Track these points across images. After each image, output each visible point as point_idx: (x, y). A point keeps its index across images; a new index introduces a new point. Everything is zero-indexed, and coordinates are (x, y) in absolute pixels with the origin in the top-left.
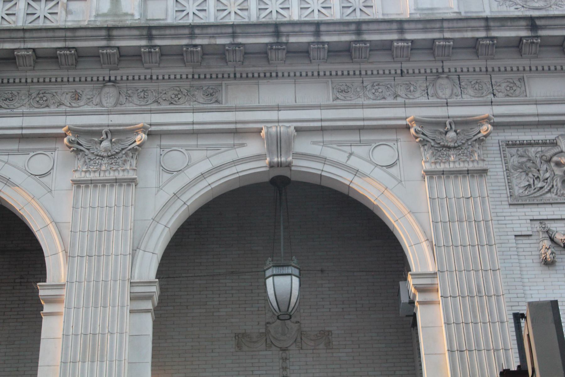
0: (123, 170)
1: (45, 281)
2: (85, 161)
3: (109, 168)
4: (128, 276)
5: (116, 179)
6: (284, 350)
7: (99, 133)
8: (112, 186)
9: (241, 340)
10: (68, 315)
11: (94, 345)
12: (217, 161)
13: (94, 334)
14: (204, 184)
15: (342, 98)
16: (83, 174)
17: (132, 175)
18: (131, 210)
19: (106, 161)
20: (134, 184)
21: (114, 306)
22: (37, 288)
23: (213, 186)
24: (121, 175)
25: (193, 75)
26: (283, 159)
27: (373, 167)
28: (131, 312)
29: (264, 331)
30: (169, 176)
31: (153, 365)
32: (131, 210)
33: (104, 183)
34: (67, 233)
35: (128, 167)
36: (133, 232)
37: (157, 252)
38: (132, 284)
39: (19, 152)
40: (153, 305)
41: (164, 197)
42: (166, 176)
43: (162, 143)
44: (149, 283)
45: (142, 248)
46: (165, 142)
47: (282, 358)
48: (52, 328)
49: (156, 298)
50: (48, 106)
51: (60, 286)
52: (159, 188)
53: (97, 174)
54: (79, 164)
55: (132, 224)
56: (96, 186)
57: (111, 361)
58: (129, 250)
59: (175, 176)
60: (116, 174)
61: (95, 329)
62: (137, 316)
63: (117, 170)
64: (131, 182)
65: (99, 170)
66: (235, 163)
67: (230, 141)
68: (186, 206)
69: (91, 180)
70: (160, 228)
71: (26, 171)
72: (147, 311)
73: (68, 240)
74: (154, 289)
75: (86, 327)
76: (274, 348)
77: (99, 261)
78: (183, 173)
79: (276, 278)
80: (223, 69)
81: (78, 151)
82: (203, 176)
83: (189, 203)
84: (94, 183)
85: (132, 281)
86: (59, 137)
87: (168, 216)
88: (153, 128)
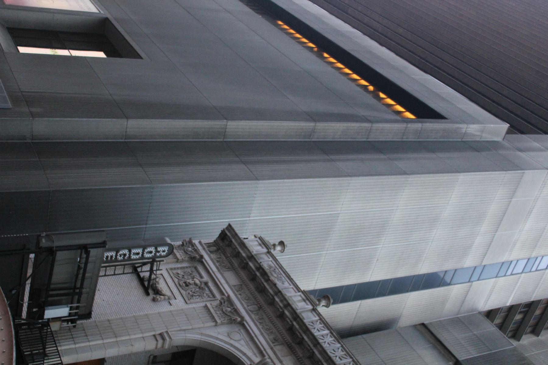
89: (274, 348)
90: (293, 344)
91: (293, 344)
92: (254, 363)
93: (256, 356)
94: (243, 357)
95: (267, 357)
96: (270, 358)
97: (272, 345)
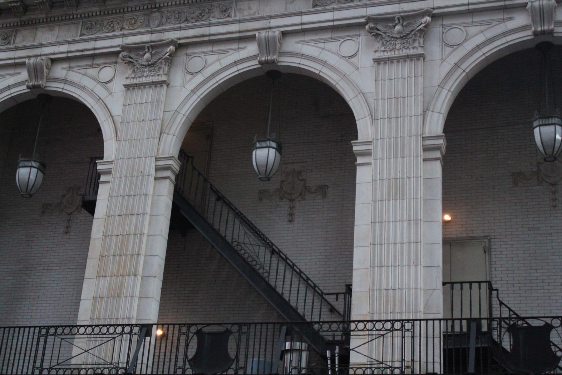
0: (413, 48)
1: (357, 139)
2: (383, 43)
3: (402, 47)
4: (420, 132)
5: (408, 56)
6: (553, 185)
7: (392, 20)
8: (405, 61)
9: (517, 177)
10: (376, 164)
11: (396, 187)
12: (490, 34)
13: (396, 179)
14: (480, 53)
15: (320, 4)
16: (382, 54)
17: (420, 51)
18: (420, 80)
19: (399, 41)
20: (422, 58)
21: (410, 157)
22: (351, 145)
23: (487, 55)
24: (411, 52)
25: (100, 12)
26: (546, 28)
27: (95, 83)
28: (424, 160)
29: (535, 170)
30: (451, 49)
31: (444, 199)
32: (420, 80)
33: (398, 59)
34: (371, 100)
35: (416, 44)
36: (423, 97)
37: (442, 112)
38: (424, 139)
39: (332, 39)
40: (441, 153)
41: (447, 67)
42: (449, 50)
43: (188, 52)
44: (438, 137)
45: (431, 109)
46: (446, 22)
47: (290, 207)
48: (363, 175)
49: (444, 149)
50: (114, 31)
51: (370, 143)
52: (443, 60)
53: (393, 53)
54: (378, 45)
55: (422, 91)
56: (392, 62)
57: (410, 199)
58: (420, 112)
59: (456, 49)
60: (408, 51)
61: (396, 174)
62: (429, 164)
63: (408, 48)
64: (420, 57)
65: (394, 49)
66: (505, 34)
67: (500, 16)
68: (465, 74)
69: (388, 58)
70: (445, 92)
71: (338, 54)
72: (436, 159)
73: (373, 106)
74: (441, 141)
75: (390, 174)
76: (285, 200)
77: (397, 122)
78: (461, 47)
79: (542, 128)
80: (90, 9)
81: (377, 36)
82: (478, 47)
83: (467, 71)
84: (390, 60)
85: (424, 136)
86: (360, 26)
87: (450, 83)
88: (436, 11)
89: (17, 45)
90: (24, 18)
91: (24, 18)
92: (27, 81)
93: (19, 73)
94: (12, 91)
95: (27, 61)
96: (29, 57)
97: (11, 46)
